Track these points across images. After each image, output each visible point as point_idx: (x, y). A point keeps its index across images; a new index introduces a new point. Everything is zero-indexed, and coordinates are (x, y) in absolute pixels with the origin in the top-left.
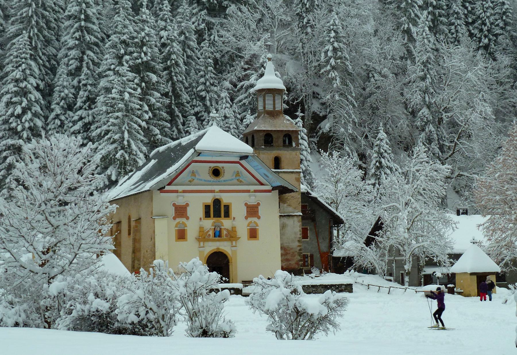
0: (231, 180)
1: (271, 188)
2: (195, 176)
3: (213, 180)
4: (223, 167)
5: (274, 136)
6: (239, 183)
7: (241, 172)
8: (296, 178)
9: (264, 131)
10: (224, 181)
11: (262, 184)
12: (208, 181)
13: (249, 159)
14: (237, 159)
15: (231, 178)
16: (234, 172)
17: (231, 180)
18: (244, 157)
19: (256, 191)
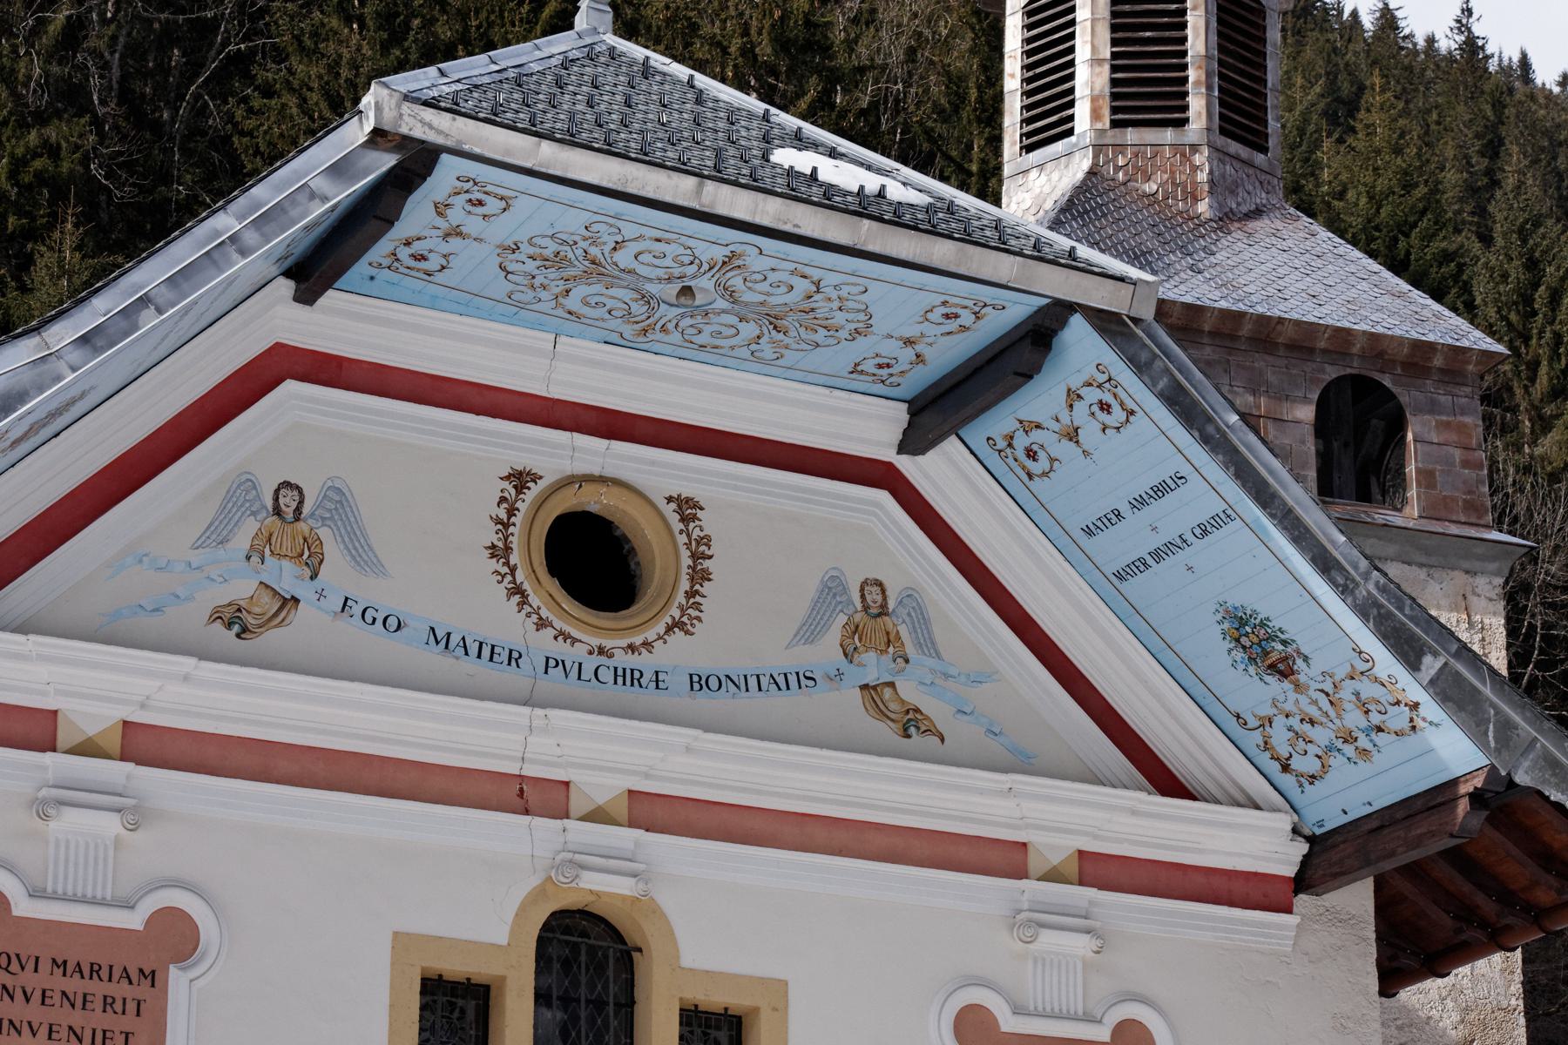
0: (782, 682)
1: (1284, 858)
2: (311, 559)
3: (545, 643)
4: (687, 508)
6: (885, 732)
10: (699, 682)
12: (488, 651)
15: (779, 659)
16: (832, 588)
17: (782, 682)
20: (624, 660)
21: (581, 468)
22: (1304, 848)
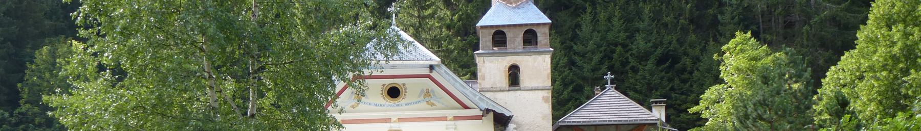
4: (404, 85)
5: (509, 35)
6: (429, 106)
7: (433, 91)
8: (543, 97)
9: (492, 27)
11: (466, 107)
13: (437, 68)
14: (427, 72)
16: (422, 91)
18: (431, 67)
19: (456, 118)
20: (397, 103)
21: (391, 83)
22: (482, 112)
